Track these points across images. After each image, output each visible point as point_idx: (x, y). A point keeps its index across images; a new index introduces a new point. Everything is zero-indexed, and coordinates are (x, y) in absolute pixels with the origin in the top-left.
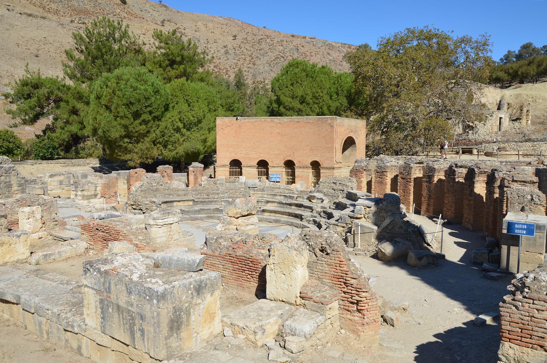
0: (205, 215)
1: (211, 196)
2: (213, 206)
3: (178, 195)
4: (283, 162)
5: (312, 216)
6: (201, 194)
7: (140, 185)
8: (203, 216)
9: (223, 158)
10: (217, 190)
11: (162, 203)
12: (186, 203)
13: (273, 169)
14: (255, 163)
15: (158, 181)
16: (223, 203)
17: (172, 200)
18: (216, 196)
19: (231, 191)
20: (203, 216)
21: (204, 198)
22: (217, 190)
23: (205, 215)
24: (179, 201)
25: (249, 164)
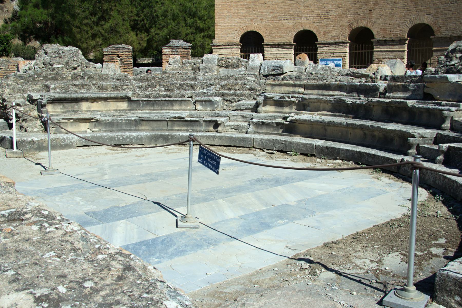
0: (148, 134)
1: (178, 91)
2: (170, 113)
3: (102, 88)
4: (347, 33)
5: (438, 140)
6: (153, 86)
7: (27, 68)
8: (143, 134)
9: (227, 28)
10: (194, 79)
11: (49, 102)
12: (112, 106)
13: (326, 49)
14: (290, 38)
15: (66, 59)
16: (199, 107)
17: (74, 96)
18: (189, 92)
19: (224, 83)
20: (143, 134)
21: (160, 96)
22: (194, 79)
23: (148, 134)
24: (94, 100)
25: (278, 40)
